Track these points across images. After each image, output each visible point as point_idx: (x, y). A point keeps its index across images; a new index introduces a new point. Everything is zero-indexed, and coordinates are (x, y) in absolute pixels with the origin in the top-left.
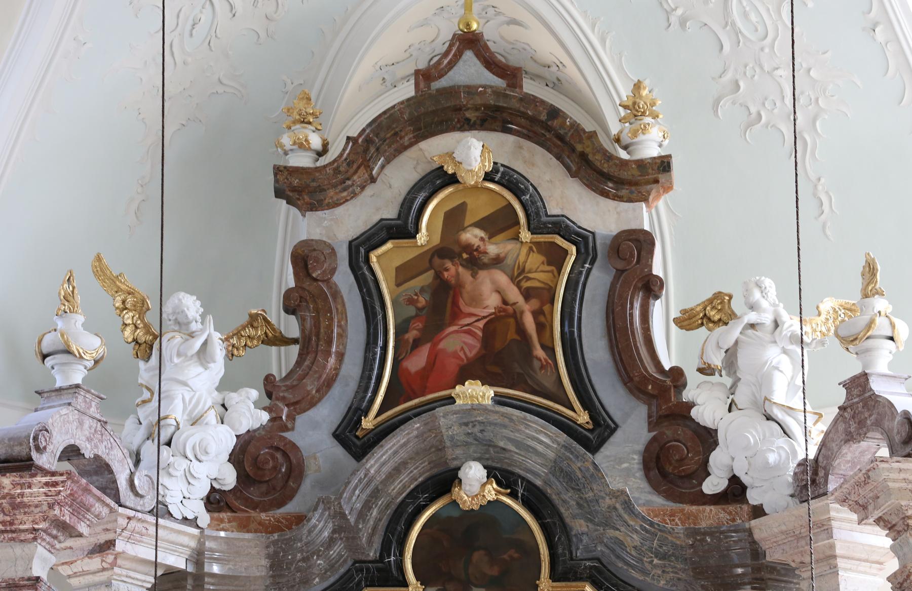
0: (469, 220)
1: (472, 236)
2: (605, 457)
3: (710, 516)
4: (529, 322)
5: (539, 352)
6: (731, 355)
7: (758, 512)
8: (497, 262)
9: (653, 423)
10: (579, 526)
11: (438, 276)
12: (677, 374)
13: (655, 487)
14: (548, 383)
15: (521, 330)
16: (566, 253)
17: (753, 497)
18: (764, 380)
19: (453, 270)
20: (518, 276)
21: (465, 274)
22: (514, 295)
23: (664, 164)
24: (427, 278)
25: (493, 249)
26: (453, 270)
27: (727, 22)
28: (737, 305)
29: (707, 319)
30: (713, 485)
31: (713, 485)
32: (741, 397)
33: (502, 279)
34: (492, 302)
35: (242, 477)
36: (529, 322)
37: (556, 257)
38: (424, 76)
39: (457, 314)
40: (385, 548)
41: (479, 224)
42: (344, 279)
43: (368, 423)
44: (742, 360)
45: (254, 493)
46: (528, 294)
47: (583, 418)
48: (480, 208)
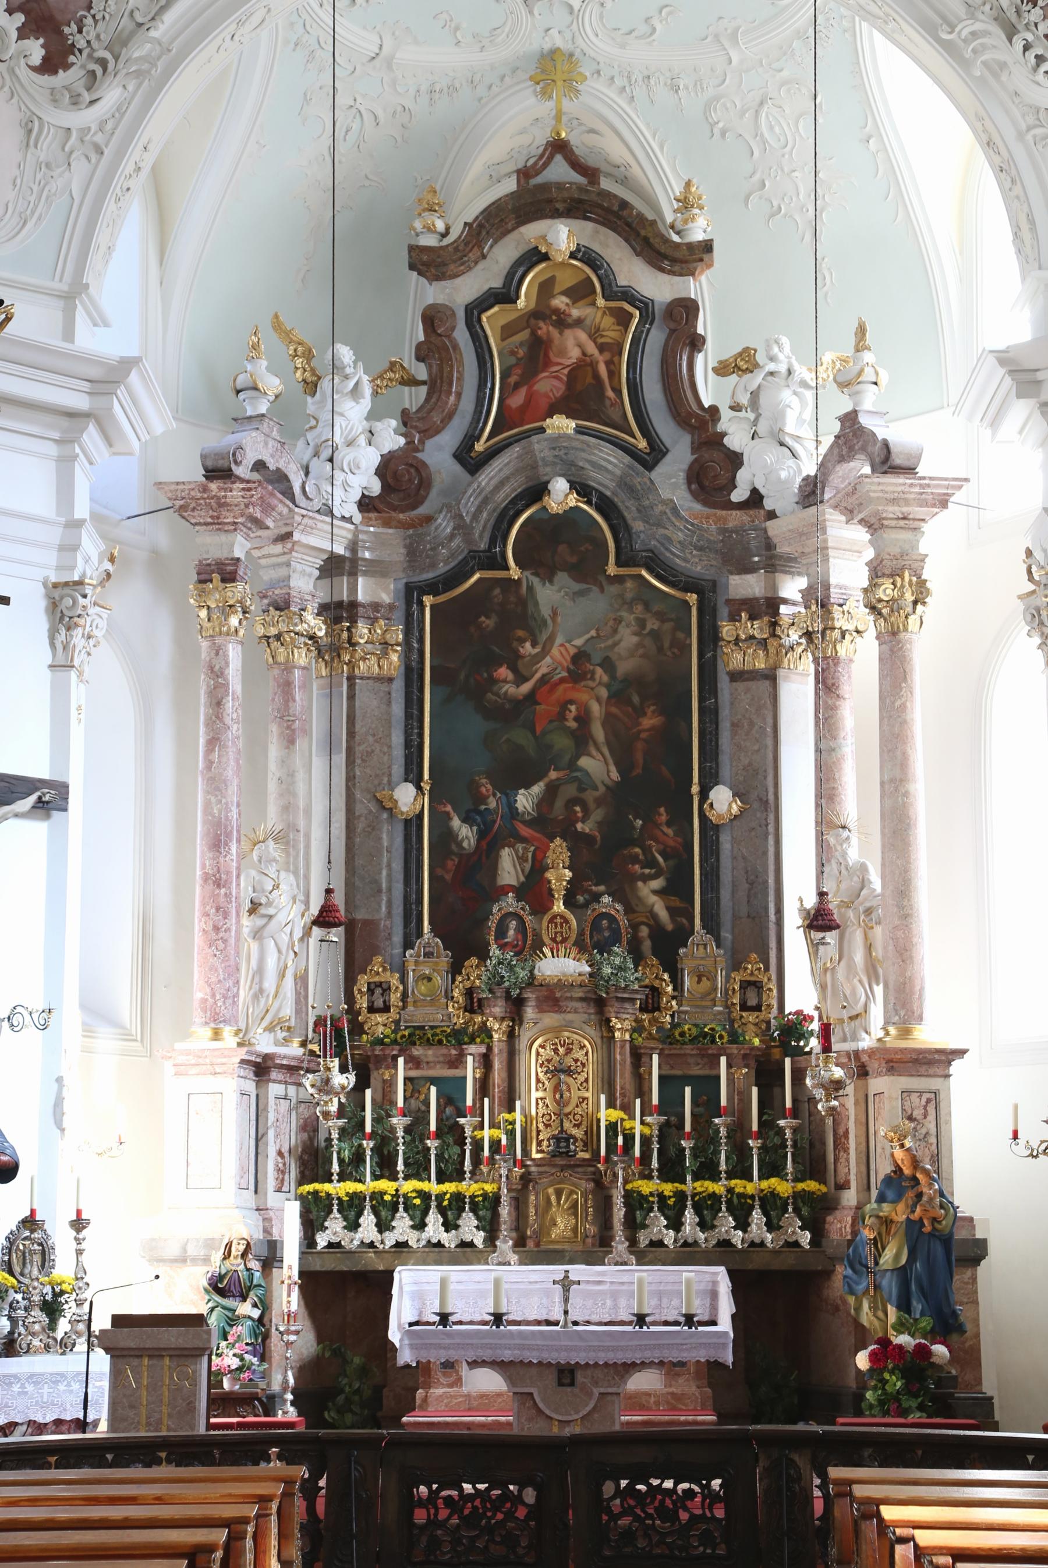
0: (558, 289)
1: (560, 302)
2: (658, 474)
3: (735, 518)
4: (602, 370)
5: (610, 393)
6: (755, 395)
7: (772, 515)
8: (579, 322)
9: (694, 449)
10: (638, 526)
11: (533, 333)
12: (714, 411)
13: (695, 495)
14: (616, 417)
15: (596, 376)
16: (631, 316)
17: (768, 504)
18: (779, 416)
19: (545, 329)
20: (594, 334)
21: (554, 332)
22: (592, 349)
23: (707, 247)
24: (524, 335)
25: (575, 313)
26: (545, 329)
27: (757, 134)
28: (760, 358)
29: (737, 369)
30: (738, 495)
31: (738, 495)
32: (762, 428)
33: (583, 336)
34: (575, 354)
35: (385, 486)
36: (602, 370)
37: (624, 319)
38: (524, 174)
39: (547, 363)
40: (493, 542)
41: (566, 293)
42: (461, 335)
43: (480, 447)
44: (763, 400)
45: (394, 499)
46: (602, 348)
47: (642, 444)
48: (566, 280)
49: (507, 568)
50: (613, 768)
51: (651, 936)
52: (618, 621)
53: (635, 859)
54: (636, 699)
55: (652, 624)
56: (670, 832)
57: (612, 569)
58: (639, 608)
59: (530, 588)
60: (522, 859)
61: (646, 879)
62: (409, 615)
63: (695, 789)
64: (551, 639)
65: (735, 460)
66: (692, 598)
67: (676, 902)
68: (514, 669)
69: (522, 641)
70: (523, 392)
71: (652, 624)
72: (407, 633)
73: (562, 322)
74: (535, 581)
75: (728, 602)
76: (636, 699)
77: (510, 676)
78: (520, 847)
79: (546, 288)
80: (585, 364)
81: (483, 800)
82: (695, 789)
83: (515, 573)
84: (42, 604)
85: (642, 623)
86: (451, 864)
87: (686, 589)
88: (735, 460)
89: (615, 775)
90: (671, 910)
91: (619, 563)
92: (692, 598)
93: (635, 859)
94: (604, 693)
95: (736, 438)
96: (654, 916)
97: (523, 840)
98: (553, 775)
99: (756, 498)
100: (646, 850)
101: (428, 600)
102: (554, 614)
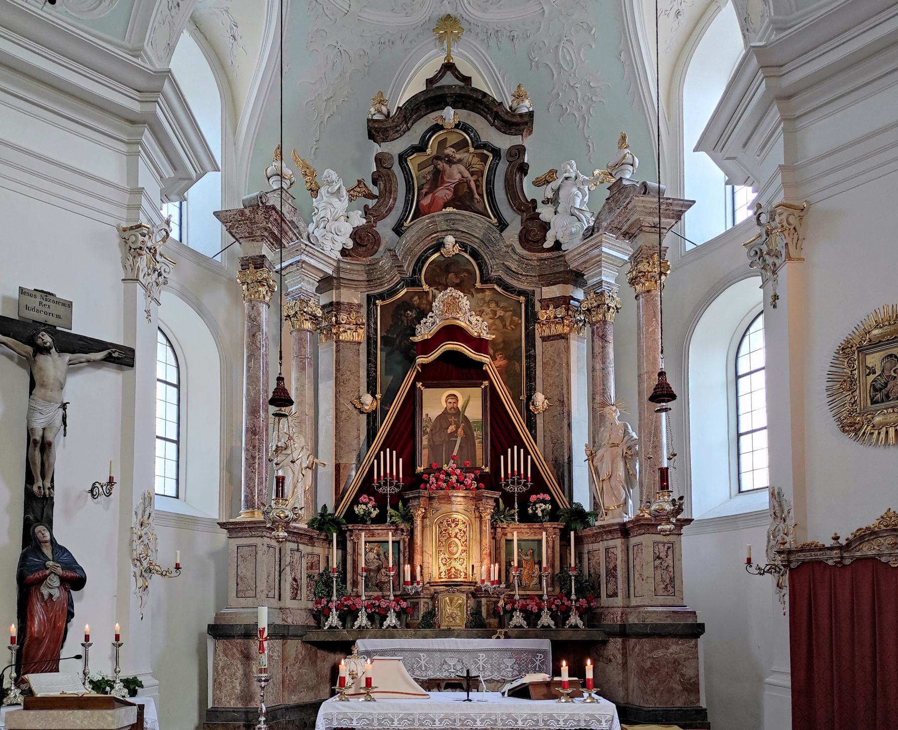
0: (448, 144)
1: (449, 151)
5: (477, 196)
8: (460, 161)
11: (435, 167)
14: (481, 209)
15: (469, 188)
19: (441, 165)
20: (468, 167)
21: (447, 166)
22: (467, 174)
24: (431, 168)
25: (458, 156)
26: (441, 165)
30: (548, 244)
31: (548, 244)
34: (458, 177)
39: (443, 182)
40: (414, 272)
42: (397, 169)
46: (472, 174)
48: (453, 139)
55: (500, 313)
57: (478, 285)
58: (493, 305)
65: (546, 226)
66: (522, 299)
70: (430, 196)
71: (500, 313)
73: (450, 161)
79: (442, 144)
80: (463, 182)
83: (426, 287)
84: (116, 241)
85: (494, 313)
88: (546, 226)
91: (483, 281)
92: (522, 299)
95: (545, 213)
99: (558, 245)
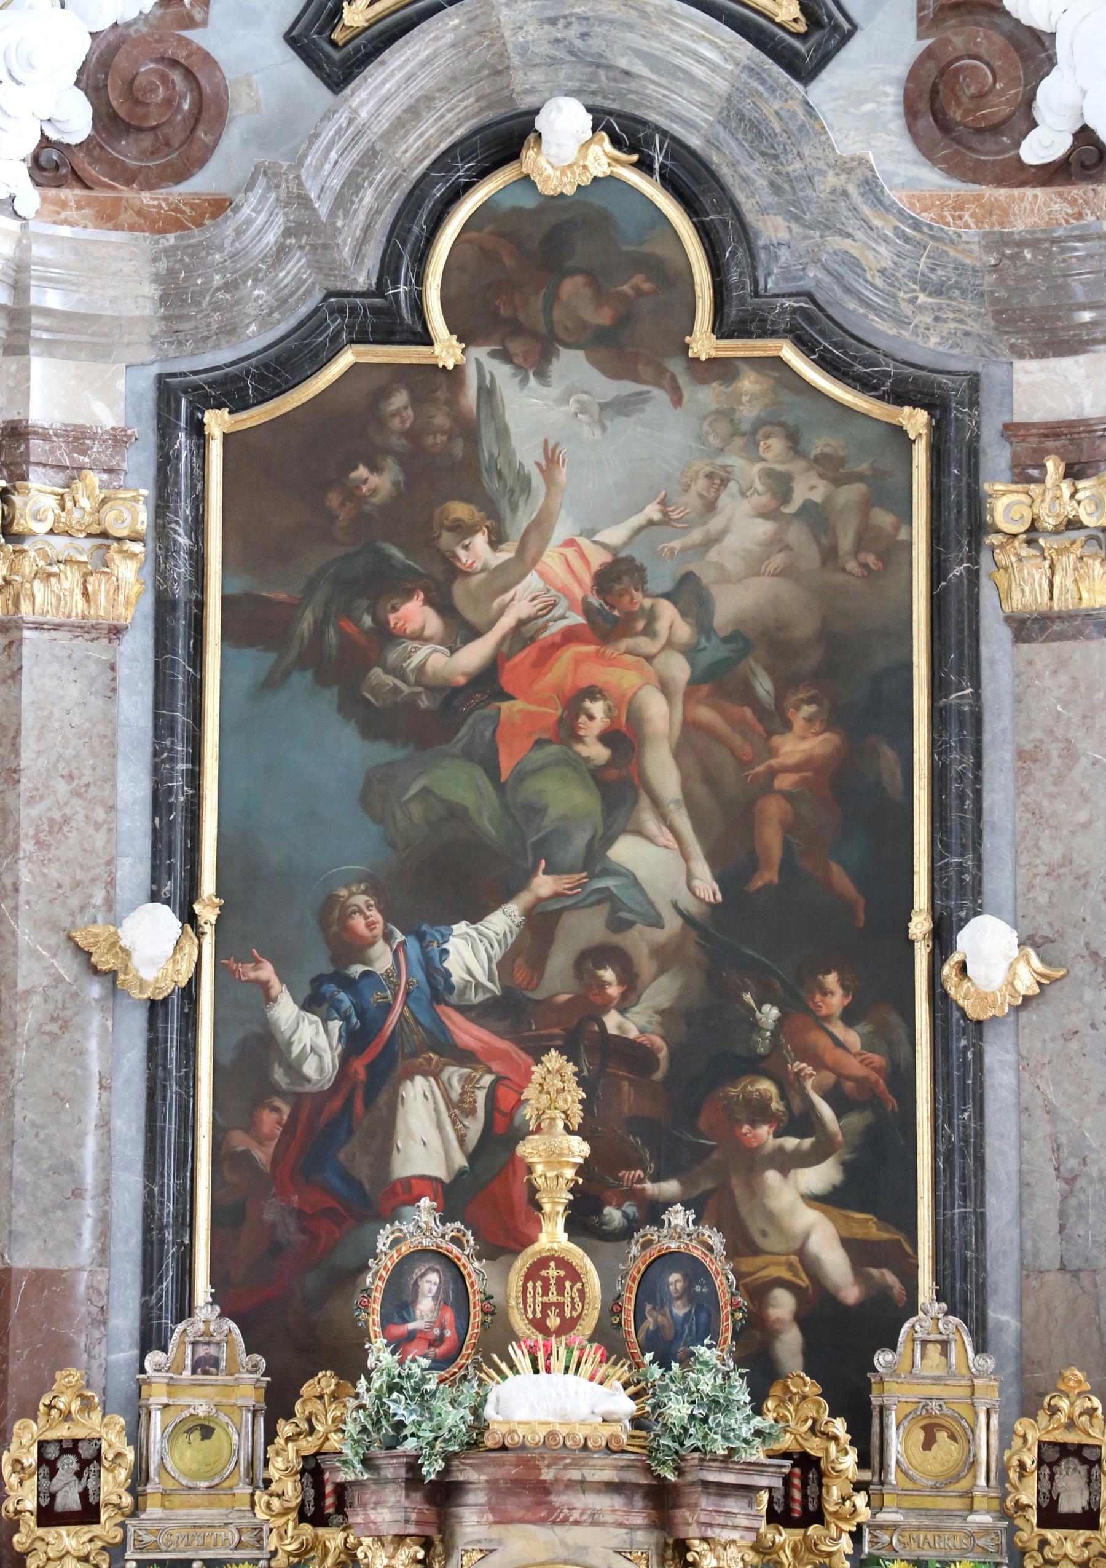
13: (927, 151)
40: (389, 268)
49: (425, 339)
50: (702, 869)
51: (801, 1319)
52: (720, 480)
53: (759, 1111)
54: (764, 686)
56: (852, 1038)
58: (775, 446)
59: (487, 393)
60: (460, 1108)
61: (787, 1163)
62: (165, 462)
63: (920, 925)
64: (541, 526)
67: (868, 1226)
68: (444, 607)
69: (464, 530)
72: (163, 507)
74: (501, 372)
75: (1011, 430)
76: (764, 686)
77: (433, 623)
78: (454, 1074)
81: (358, 949)
82: (920, 925)
86: (270, 1121)
87: (900, 396)
89: (708, 887)
90: (854, 1248)
91: (721, 328)
93: (759, 1111)
94: (679, 669)
96: (808, 1263)
97: (464, 1057)
98: (544, 885)
100: (788, 1086)
101: (217, 422)
102: (551, 460)
